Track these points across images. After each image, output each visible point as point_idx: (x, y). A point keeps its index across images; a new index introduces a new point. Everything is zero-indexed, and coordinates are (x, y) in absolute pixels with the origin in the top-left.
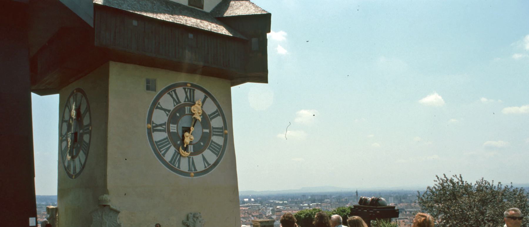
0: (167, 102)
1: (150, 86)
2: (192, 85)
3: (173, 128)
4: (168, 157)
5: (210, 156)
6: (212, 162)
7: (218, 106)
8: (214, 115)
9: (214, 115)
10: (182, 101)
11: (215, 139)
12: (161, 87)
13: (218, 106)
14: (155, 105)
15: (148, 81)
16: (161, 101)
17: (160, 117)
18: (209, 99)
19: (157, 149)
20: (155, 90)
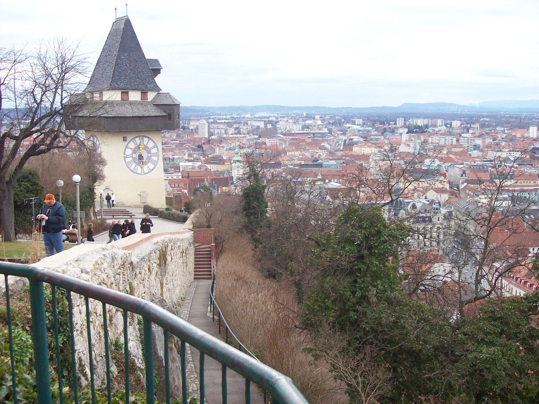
0: (132, 145)
1: (125, 139)
2: (143, 136)
3: (134, 156)
4: (132, 168)
5: (151, 166)
6: (151, 168)
7: (155, 143)
8: (153, 147)
9: (153, 147)
10: (138, 144)
11: (153, 158)
12: (129, 139)
13: (155, 143)
14: (127, 147)
15: (124, 138)
16: (129, 145)
17: (129, 152)
18: (150, 141)
19: (127, 165)
20: (126, 141)
